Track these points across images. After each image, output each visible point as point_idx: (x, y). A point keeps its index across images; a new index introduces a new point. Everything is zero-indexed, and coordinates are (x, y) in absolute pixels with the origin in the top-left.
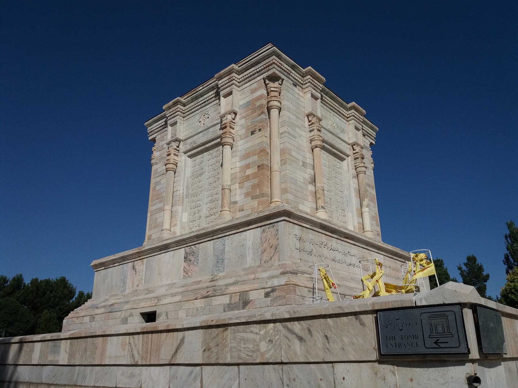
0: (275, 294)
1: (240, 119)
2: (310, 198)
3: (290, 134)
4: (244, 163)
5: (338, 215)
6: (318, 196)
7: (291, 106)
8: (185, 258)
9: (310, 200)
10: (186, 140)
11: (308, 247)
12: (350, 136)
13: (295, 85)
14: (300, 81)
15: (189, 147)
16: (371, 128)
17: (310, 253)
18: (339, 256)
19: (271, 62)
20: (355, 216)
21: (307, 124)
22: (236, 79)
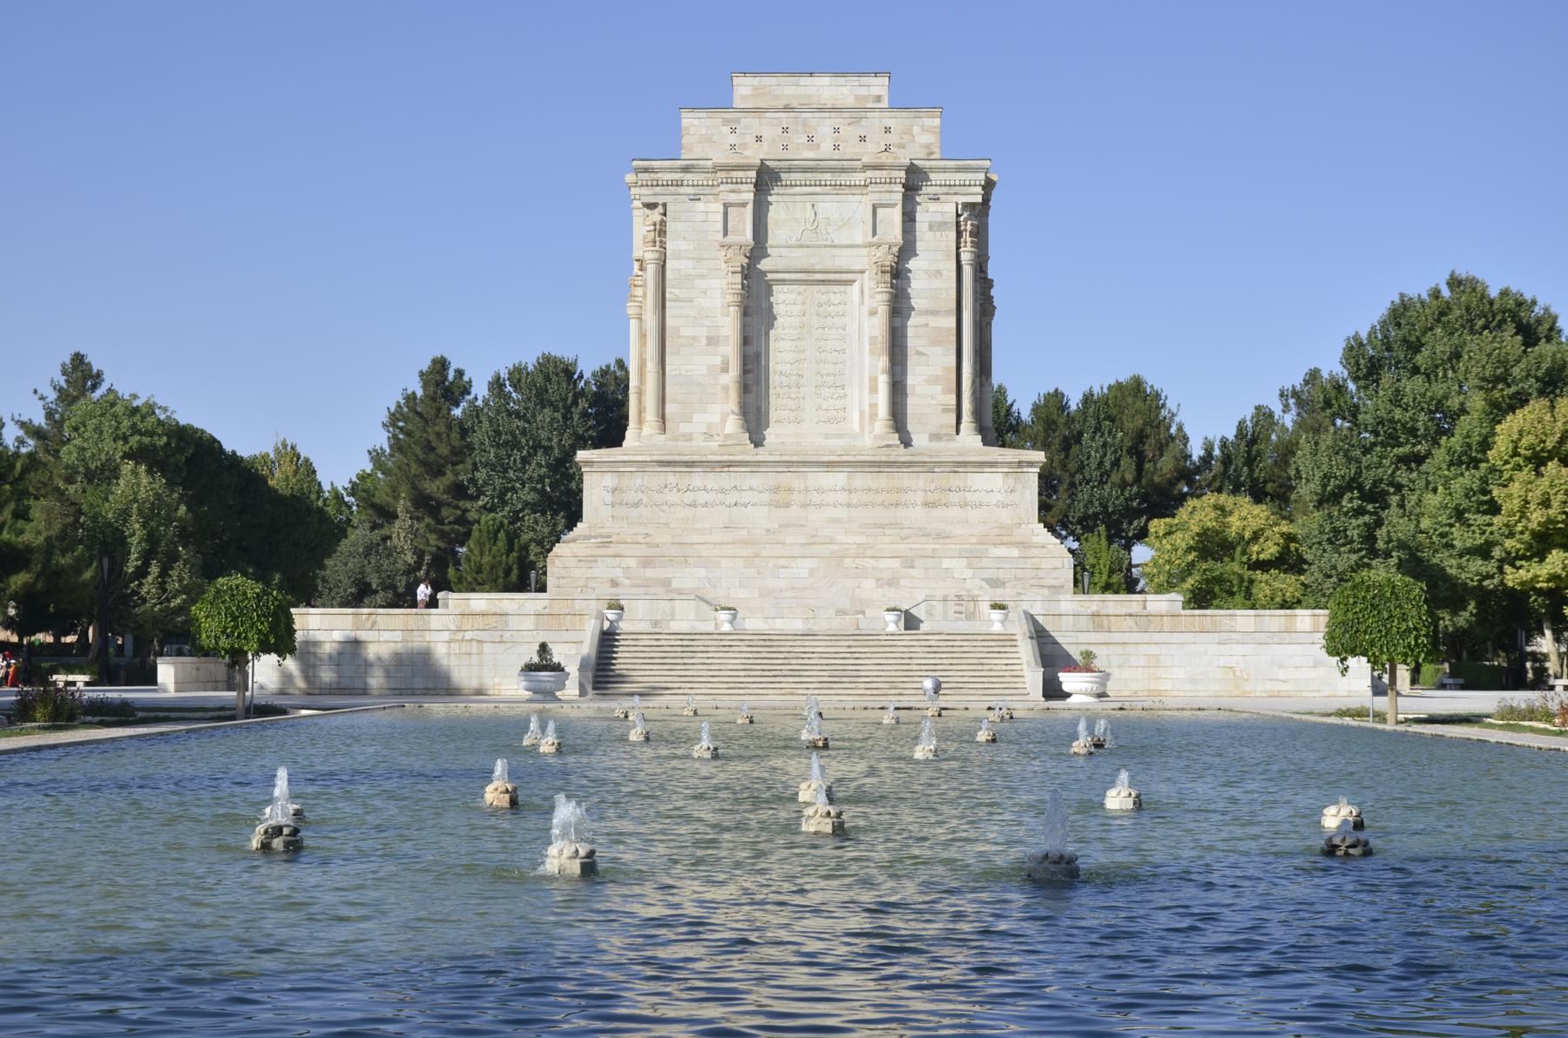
7: (683, 246)
11: (633, 497)
17: (636, 505)
18: (702, 497)
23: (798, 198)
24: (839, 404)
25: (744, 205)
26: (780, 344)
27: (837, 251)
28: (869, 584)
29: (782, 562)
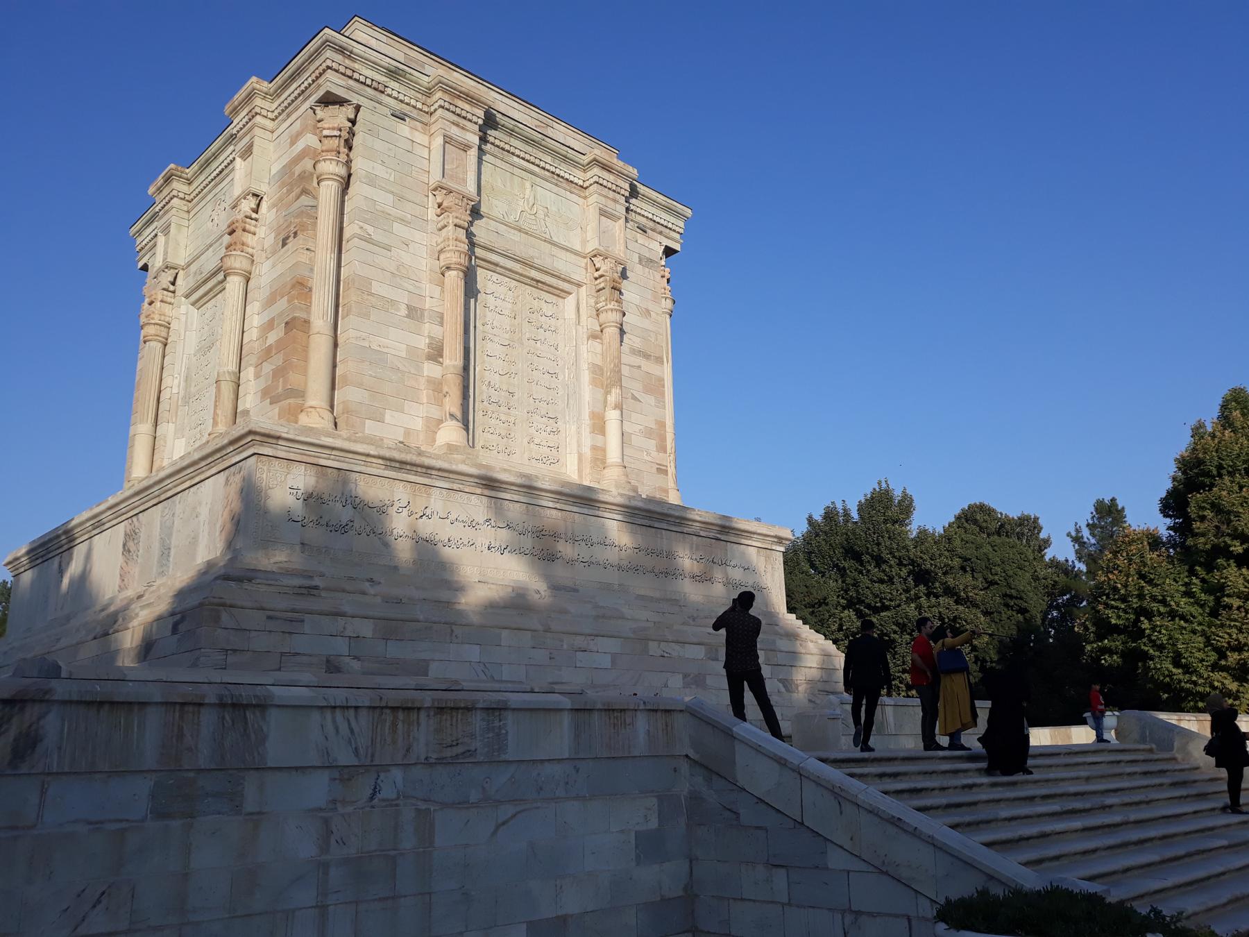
0: (182, 628)
1: (270, 209)
2: (424, 395)
3: (369, 240)
4: (266, 317)
5: (533, 431)
6: (445, 389)
7: (380, 171)
8: (124, 545)
9: (425, 400)
10: (189, 265)
12: (590, 235)
13: (401, 117)
14: (419, 105)
15: (192, 283)
16: (668, 210)
19: (324, 66)
20: (586, 431)
21: (432, 212)
22: (264, 112)
23: (517, 171)
24: (553, 439)
25: (465, 147)
26: (489, 344)
27: (555, 250)
28: (676, 681)
29: (579, 641)
